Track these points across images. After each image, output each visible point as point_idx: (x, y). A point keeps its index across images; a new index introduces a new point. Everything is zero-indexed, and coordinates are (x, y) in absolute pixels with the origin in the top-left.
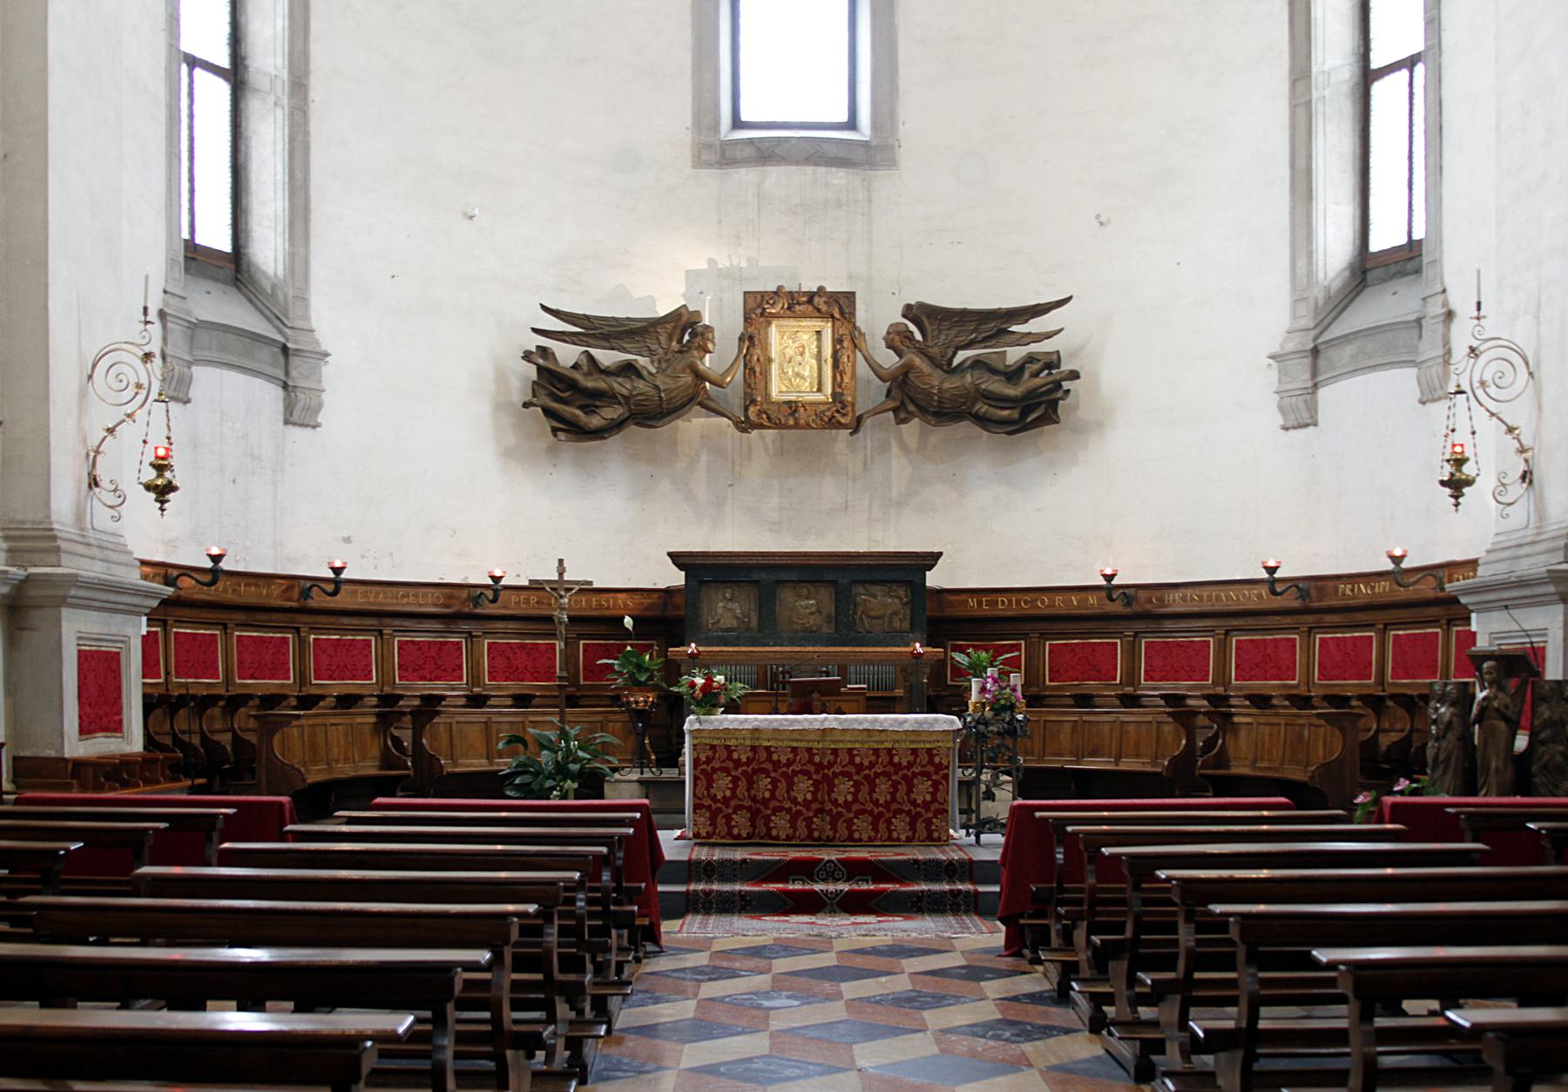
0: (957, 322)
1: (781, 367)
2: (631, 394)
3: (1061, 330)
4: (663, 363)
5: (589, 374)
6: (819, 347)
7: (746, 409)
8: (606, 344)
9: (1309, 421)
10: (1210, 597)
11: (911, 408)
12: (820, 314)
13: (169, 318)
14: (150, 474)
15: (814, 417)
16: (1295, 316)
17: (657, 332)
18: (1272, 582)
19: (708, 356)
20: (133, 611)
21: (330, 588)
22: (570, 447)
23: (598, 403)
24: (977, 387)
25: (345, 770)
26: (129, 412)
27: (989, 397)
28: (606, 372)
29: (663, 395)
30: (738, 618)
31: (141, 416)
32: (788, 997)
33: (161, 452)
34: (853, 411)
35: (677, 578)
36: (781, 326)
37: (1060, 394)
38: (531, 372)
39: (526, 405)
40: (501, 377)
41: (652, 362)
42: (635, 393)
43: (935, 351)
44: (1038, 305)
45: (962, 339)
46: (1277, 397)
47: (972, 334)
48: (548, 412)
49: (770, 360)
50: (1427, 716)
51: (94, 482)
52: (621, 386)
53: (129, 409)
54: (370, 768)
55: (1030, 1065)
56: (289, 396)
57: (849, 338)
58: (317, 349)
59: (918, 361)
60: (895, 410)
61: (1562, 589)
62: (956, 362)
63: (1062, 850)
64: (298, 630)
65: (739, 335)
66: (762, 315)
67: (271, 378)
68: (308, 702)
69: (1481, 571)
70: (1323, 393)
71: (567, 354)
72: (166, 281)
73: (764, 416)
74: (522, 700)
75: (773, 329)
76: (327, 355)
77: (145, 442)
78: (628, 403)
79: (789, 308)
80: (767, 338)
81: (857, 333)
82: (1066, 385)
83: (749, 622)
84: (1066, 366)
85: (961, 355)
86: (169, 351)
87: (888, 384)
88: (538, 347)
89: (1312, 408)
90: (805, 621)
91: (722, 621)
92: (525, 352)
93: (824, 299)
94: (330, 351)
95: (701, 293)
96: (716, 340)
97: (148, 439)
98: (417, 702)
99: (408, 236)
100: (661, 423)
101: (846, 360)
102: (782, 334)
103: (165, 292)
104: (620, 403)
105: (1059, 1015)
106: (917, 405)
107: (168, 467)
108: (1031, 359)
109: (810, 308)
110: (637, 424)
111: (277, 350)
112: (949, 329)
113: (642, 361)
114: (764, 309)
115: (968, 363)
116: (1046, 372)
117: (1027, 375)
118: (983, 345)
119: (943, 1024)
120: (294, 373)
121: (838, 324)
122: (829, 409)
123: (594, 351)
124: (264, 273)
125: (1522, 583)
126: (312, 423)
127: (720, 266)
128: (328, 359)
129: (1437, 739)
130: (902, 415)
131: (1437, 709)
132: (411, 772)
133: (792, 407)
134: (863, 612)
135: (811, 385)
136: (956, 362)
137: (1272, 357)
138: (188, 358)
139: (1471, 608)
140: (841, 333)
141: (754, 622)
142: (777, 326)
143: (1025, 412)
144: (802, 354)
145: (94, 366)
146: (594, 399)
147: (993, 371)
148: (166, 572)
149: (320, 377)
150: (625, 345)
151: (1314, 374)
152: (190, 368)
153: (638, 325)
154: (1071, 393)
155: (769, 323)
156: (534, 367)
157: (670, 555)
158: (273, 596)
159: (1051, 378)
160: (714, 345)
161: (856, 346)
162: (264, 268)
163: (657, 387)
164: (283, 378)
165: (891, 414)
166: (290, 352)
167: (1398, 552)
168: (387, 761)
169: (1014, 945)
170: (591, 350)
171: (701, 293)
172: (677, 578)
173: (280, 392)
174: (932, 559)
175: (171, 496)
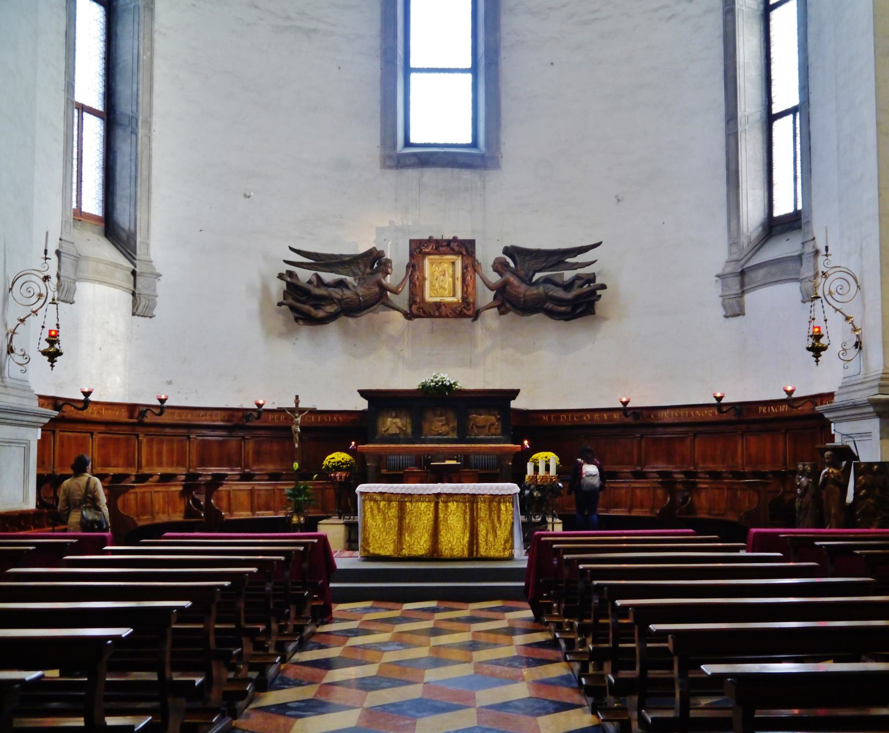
0: (535, 256)
1: (431, 282)
3: (595, 261)
4: (361, 280)
5: (318, 286)
6: (454, 271)
7: (410, 306)
8: (328, 270)
9: (740, 313)
10: (684, 415)
11: (508, 306)
12: (454, 252)
13: (62, 255)
14: (46, 346)
15: (451, 311)
17: (358, 263)
18: (719, 405)
19: (389, 275)
20: (36, 427)
21: (157, 411)
22: (305, 331)
23: (322, 303)
24: (546, 294)
25: (162, 518)
26: (34, 310)
27: (553, 299)
28: (328, 285)
29: (361, 298)
30: (400, 428)
31: (41, 312)
32: (398, 645)
33: (53, 333)
34: (474, 307)
35: (362, 405)
36: (432, 259)
37: (595, 298)
38: (283, 285)
39: (280, 304)
40: (265, 289)
41: (355, 280)
42: (344, 297)
43: (522, 273)
44: (582, 247)
45: (538, 266)
46: (720, 299)
47: (543, 264)
48: (293, 308)
49: (424, 279)
50: (795, 483)
51: (10, 350)
52: (336, 293)
53: (35, 308)
54: (178, 517)
55: (523, 680)
56: (136, 299)
57: (471, 266)
59: (512, 279)
60: (499, 307)
61: (878, 409)
62: (535, 279)
63: (556, 559)
64: (137, 436)
65: (407, 263)
66: (420, 252)
67: (126, 289)
68: (142, 478)
69: (836, 399)
70: (747, 297)
71: (305, 275)
72: (61, 233)
73: (421, 311)
74: (274, 477)
75: (427, 262)
76: (161, 275)
77: (43, 327)
79: (437, 248)
80: (423, 266)
81: (476, 263)
82: (599, 292)
83: (406, 430)
84: (599, 281)
85: (537, 276)
86: (62, 273)
87: (495, 292)
88: (287, 271)
90: (439, 430)
91: (390, 429)
92: (279, 274)
93: (456, 244)
94: (162, 274)
95: (385, 240)
96: (393, 267)
97: (45, 325)
98: (209, 478)
99: (211, 208)
100: (359, 314)
101: (469, 278)
102: (432, 263)
103: (60, 239)
104: (335, 303)
105: (550, 653)
106: (510, 303)
107: (58, 342)
108: (578, 277)
109: (449, 249)
110: (346, 315)
111: (129, 273)
112: (530, 260)
113: (350, 279)
114: (421, 250)
115: (541, 280)
116: (587, 285)
117: (576, 286)
118: (550, 270)
119: (482, 659)
120: (139, 286)
121: (465, 258)
122: (459, 306)
123: (320, 273)
124: (123, 229)
125: (855, 406)
127: (396, 225)
128: (160, 278)
129: (802, 496)
130: (503, 309)
131: (800, 479)
132: (204, 520)
133: (438, 305)
134: (473, 424)
135: (449, 292)
136: (535, 279)
137: (718, 276)
138: (73, 277)
139: (831, 420)
140: (466, 262)
141: (409, 431)
142: (428, 259)
143: (576, 307)
144: (444, 275)
145: (13, 283)
146: (319, 301)
147: (556, 284)
148: (55, 402)
149: (155, 288)
150: (339, 270)
151: (742, 285)
152: (74, 283)
153: (347, 259)
154: (602, 297)
155: (424, 258)
158: (123, 416)
159: (589, 289)
160: (392, 270)
161: (475, 271)
162: (123, 226)
163: (357, 294)
165: (495, 310)
166: (137, 274)
167: (789, 388)
168: (188, 512)
169: (538, 618)
170: (319, 273)
171: (385, 240)
172: (362, 405)
173: (131, 297)
174: (514, 393)
175: (58, 358)
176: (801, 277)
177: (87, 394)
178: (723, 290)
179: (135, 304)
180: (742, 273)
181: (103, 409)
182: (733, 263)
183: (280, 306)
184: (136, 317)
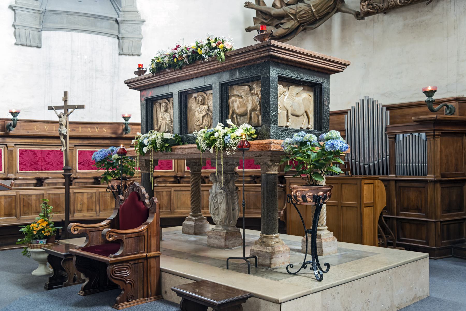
2: (296, 12)
38: (253, 13)
42: (298, 11)
58: (138, 19)
78: (296, 19)
92: (246, 3)
111: (114, 22)
120: (122, 31)
156: (254, 11)
164: (117, 34)
173: (117, 41)
177: (14, 114)
179: (120, 47)
181: (80, 127)
183: (250, 31)
184: (123, 56)
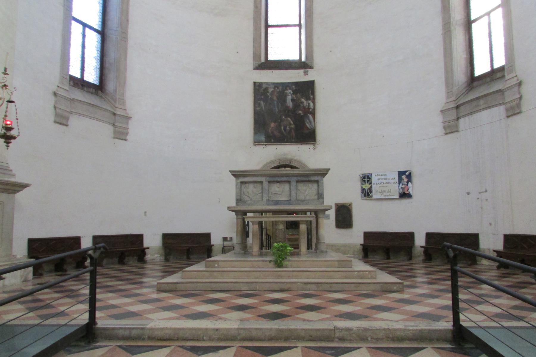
16: (448, 97)
46: (442, 124)
67: (110, 123)
70: (461, 121)
76: (131, 118)
89: (457, 126)
94: (132, 117)
126: (124, 138)
137: (441, 111)
157: (231, 171)
175: (12, 141)
176: (505, 102)
178: (443, 118)
179: (115, 132)
180: (457, 107)
182: (452, 103)
